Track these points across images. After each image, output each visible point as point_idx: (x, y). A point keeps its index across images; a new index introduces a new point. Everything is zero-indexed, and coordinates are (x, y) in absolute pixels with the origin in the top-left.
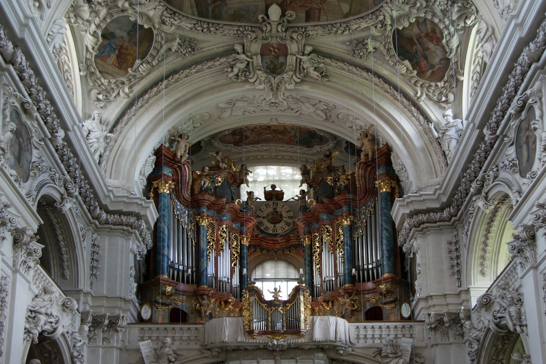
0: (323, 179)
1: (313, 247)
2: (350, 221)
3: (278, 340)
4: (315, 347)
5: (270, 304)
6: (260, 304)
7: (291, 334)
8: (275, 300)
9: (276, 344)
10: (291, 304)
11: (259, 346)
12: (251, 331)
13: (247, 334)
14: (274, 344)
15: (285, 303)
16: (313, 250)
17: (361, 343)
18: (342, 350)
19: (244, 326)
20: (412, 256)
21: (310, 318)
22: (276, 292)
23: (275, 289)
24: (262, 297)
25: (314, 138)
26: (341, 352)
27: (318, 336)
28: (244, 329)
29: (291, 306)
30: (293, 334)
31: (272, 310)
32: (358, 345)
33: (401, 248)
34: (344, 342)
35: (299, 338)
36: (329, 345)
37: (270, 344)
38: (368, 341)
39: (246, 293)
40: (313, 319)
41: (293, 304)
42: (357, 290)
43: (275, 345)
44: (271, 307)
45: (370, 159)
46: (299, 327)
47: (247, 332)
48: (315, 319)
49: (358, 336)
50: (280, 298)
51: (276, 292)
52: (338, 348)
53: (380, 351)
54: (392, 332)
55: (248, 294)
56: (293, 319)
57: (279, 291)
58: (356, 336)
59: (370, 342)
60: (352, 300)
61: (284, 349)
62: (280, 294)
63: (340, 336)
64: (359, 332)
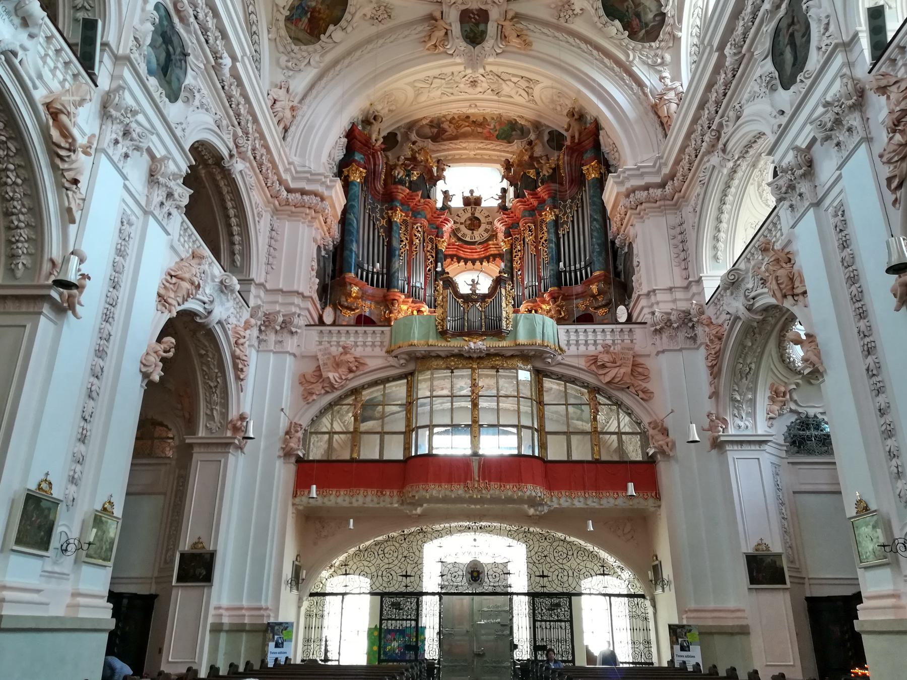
0: (525, 173)
2: (555, 215)
4: (518, 353)
5: (467, 298)
7: (490, 335)
8: (472, 294)
15: (484, 297)
17: (573, 350)
18: (550, 357)
20: (626, 250)
21: (512, 316)
22: (474, 284)
23: (473, 281)
25: (515, 130)
26: (549, 360)
27: (522, 338)
32: (568, 353)
33: (613, 243)
34: (553, 347)
36: (536, 351)
38: (580, 348)
40: (516, 317)
42: (564, 295)
45: (576, 141)
46: (500, 326)
49: (568, 341)
50: (477, 292)
51: (474, 284)
52: (545, 355)
53: (594, 360)
54: (609, 337)
57: (477, 283)
58: (566, 342)
59: (582, 348)
60: (558, 306)
61: (482, 355)
62: (478, 286)
63: (548, 341)
64: (569, 336)
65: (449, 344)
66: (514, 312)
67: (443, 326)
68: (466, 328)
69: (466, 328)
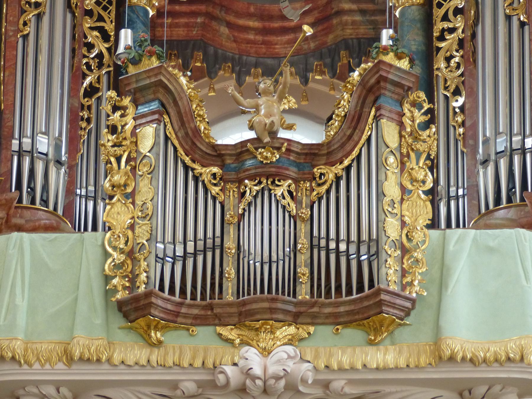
1: (438, 13)
3: (266, 352)
6: (186, 168)
9: (257, 371)
10: (339, 169)
11: (175, 385)
12: (136, 299)
13: (118, 320)
14: (248, 373)
16: (439, 26)
19: (107, 279)
24: (197, 131)
28: (109, 293)
29: (338, 179)
30: (346, 324)
31: (243, 195)
35: (371, 343)
37: (229, 370)
39: (125, 108)
41: (348, 169)
43: (254, 378)
44: (240, 182)
47: (121, 305)
48: (451, 247)
55: (131, 111)
56: (343, 247)
65: (155, 356)
66: (434, 224)
67: (133, 279)
68: (230, 288)
69: (230, 288)
